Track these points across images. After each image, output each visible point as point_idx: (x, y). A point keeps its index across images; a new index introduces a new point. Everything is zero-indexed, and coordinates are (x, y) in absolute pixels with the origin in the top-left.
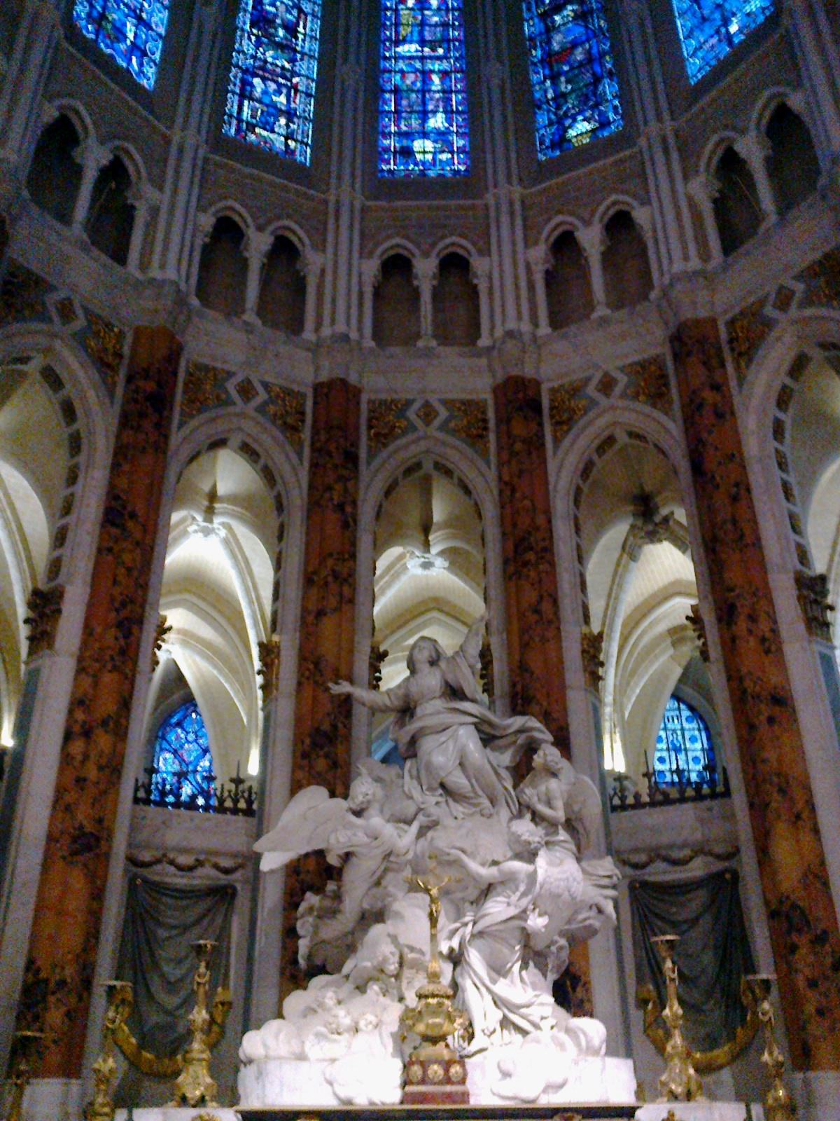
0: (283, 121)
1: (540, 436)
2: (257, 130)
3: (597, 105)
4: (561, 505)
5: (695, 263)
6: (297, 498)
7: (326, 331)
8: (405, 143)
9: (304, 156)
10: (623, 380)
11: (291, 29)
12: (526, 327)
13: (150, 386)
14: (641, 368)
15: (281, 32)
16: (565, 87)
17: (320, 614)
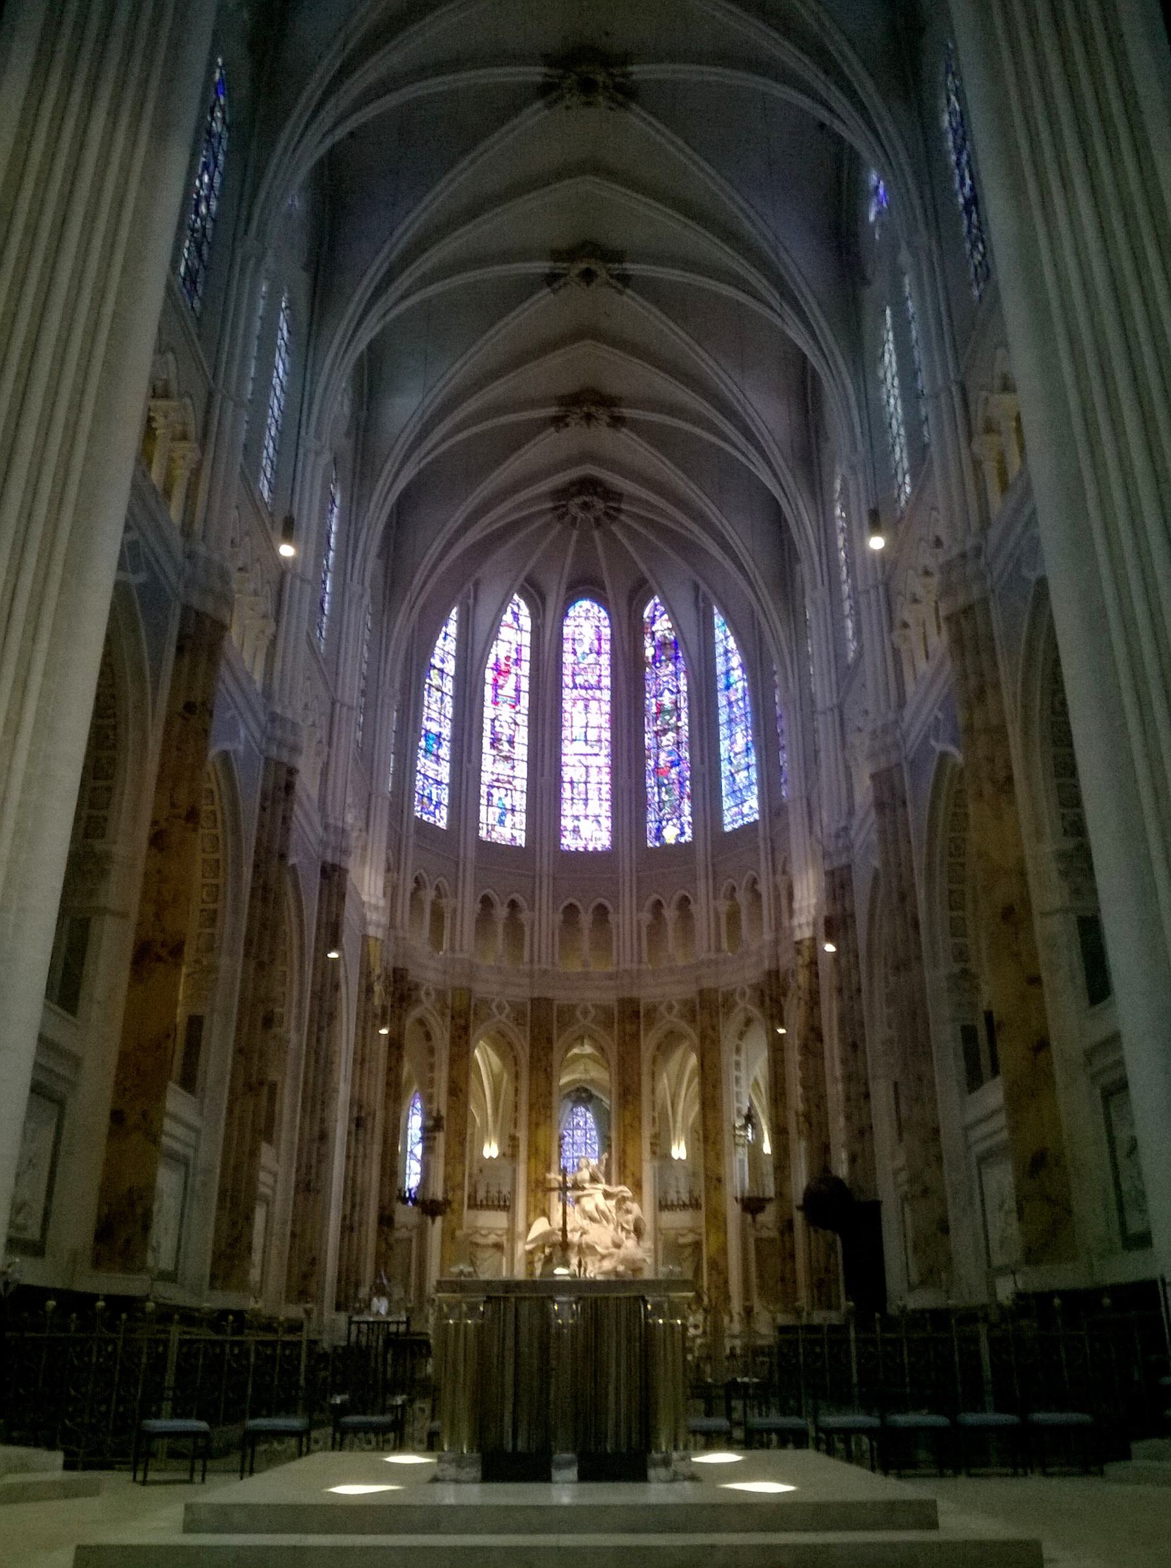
0: (509, 816)
1: (638, 1032)
2: (498, 828)
3: (679, 818)
4: (646, 1069)
5: (713, 956)
6: (524, 1060)
7: (536, 967)
8: (576, 823)
9: (521, 841)
10: (677, 1007)
11: (511, 742)
12: (635, 966)
13: (463, 1022)
14: (685, 1003)
15: (506, 747)
16: (665, 797)
17: (537, 1125)
